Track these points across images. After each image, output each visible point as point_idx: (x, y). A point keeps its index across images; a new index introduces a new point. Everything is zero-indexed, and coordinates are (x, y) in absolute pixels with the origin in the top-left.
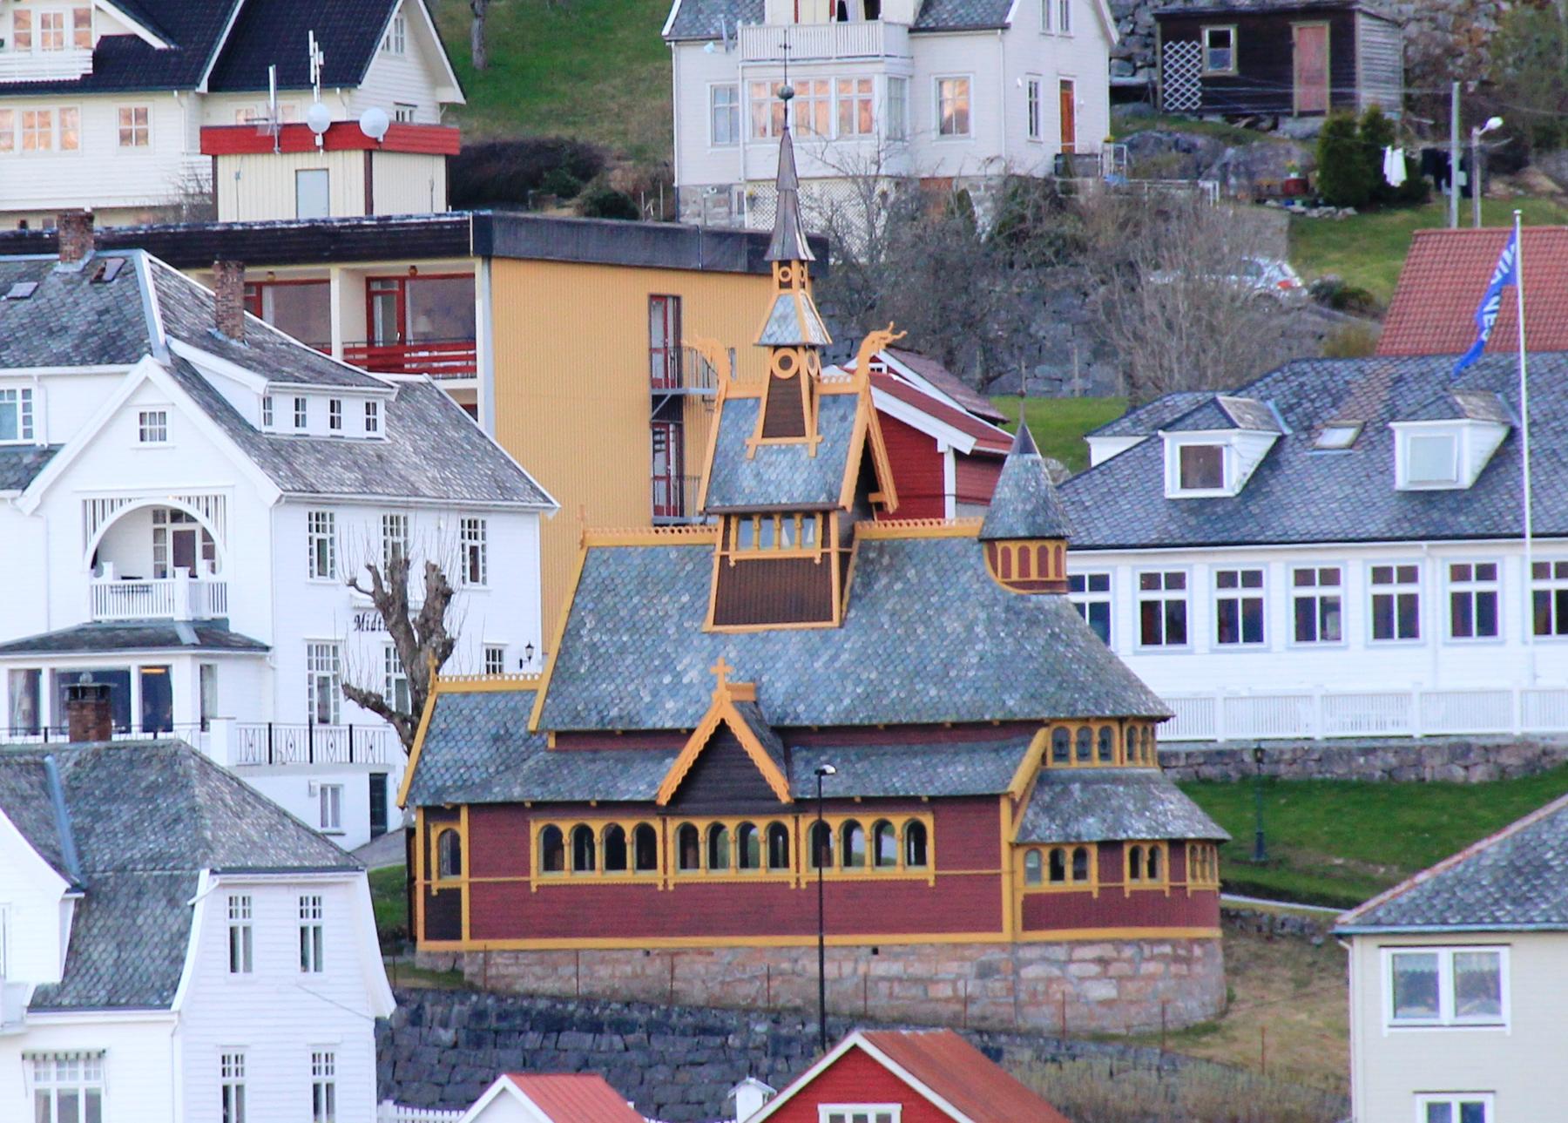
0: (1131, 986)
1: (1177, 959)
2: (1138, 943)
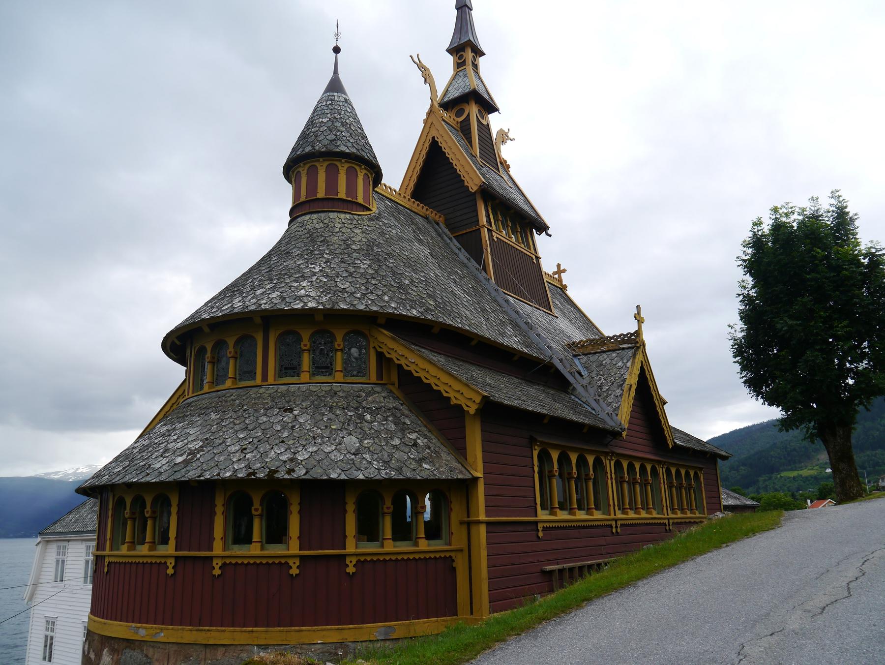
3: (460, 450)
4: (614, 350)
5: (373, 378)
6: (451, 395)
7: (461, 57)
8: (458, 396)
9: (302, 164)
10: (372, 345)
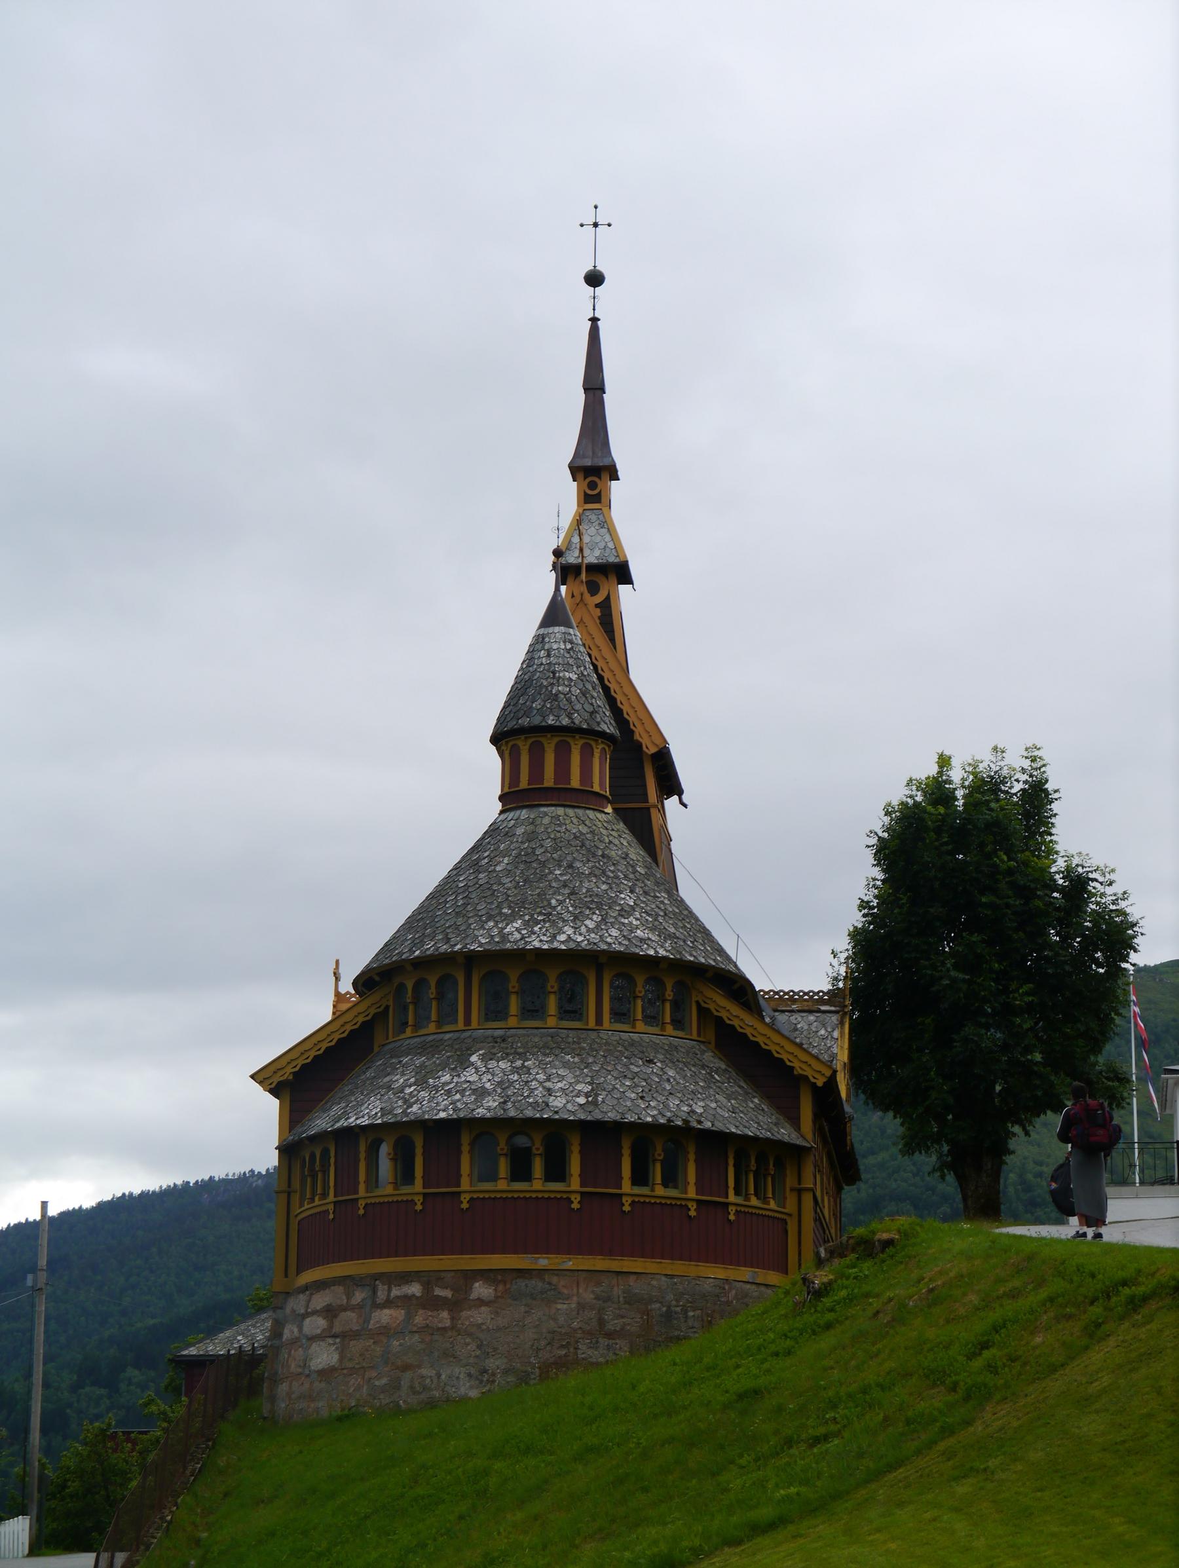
0: (356, 1346)
1: (430, 1303)
2: (370, 1281)
3: (795, 1121)
4: (810, 1012)
5: (695, 1036)
6: (796, 1064)
7: (592, 486)
8: (804, 1066)
9: (549, 735)
10: (694, 999)
